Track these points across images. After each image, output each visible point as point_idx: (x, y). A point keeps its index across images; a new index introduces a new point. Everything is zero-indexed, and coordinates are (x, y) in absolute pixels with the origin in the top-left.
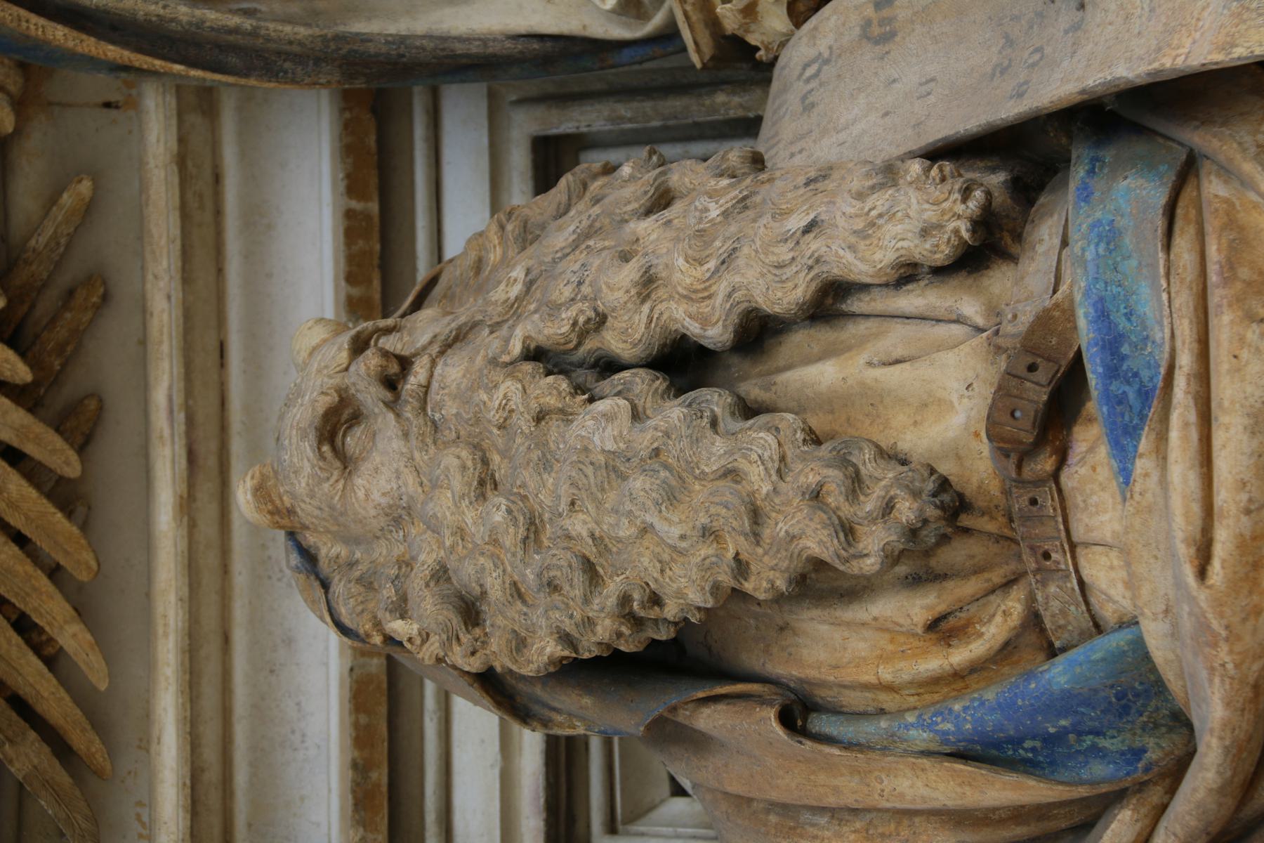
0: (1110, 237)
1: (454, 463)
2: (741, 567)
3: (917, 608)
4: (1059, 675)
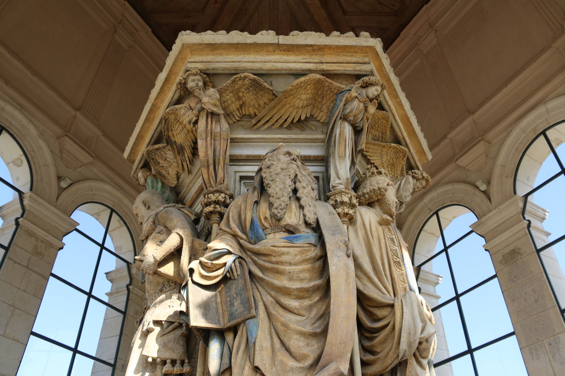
0: (308, 237)
1: (285, 166)
2: (273, 197)
3: (268, 216)
4: (261, 231)
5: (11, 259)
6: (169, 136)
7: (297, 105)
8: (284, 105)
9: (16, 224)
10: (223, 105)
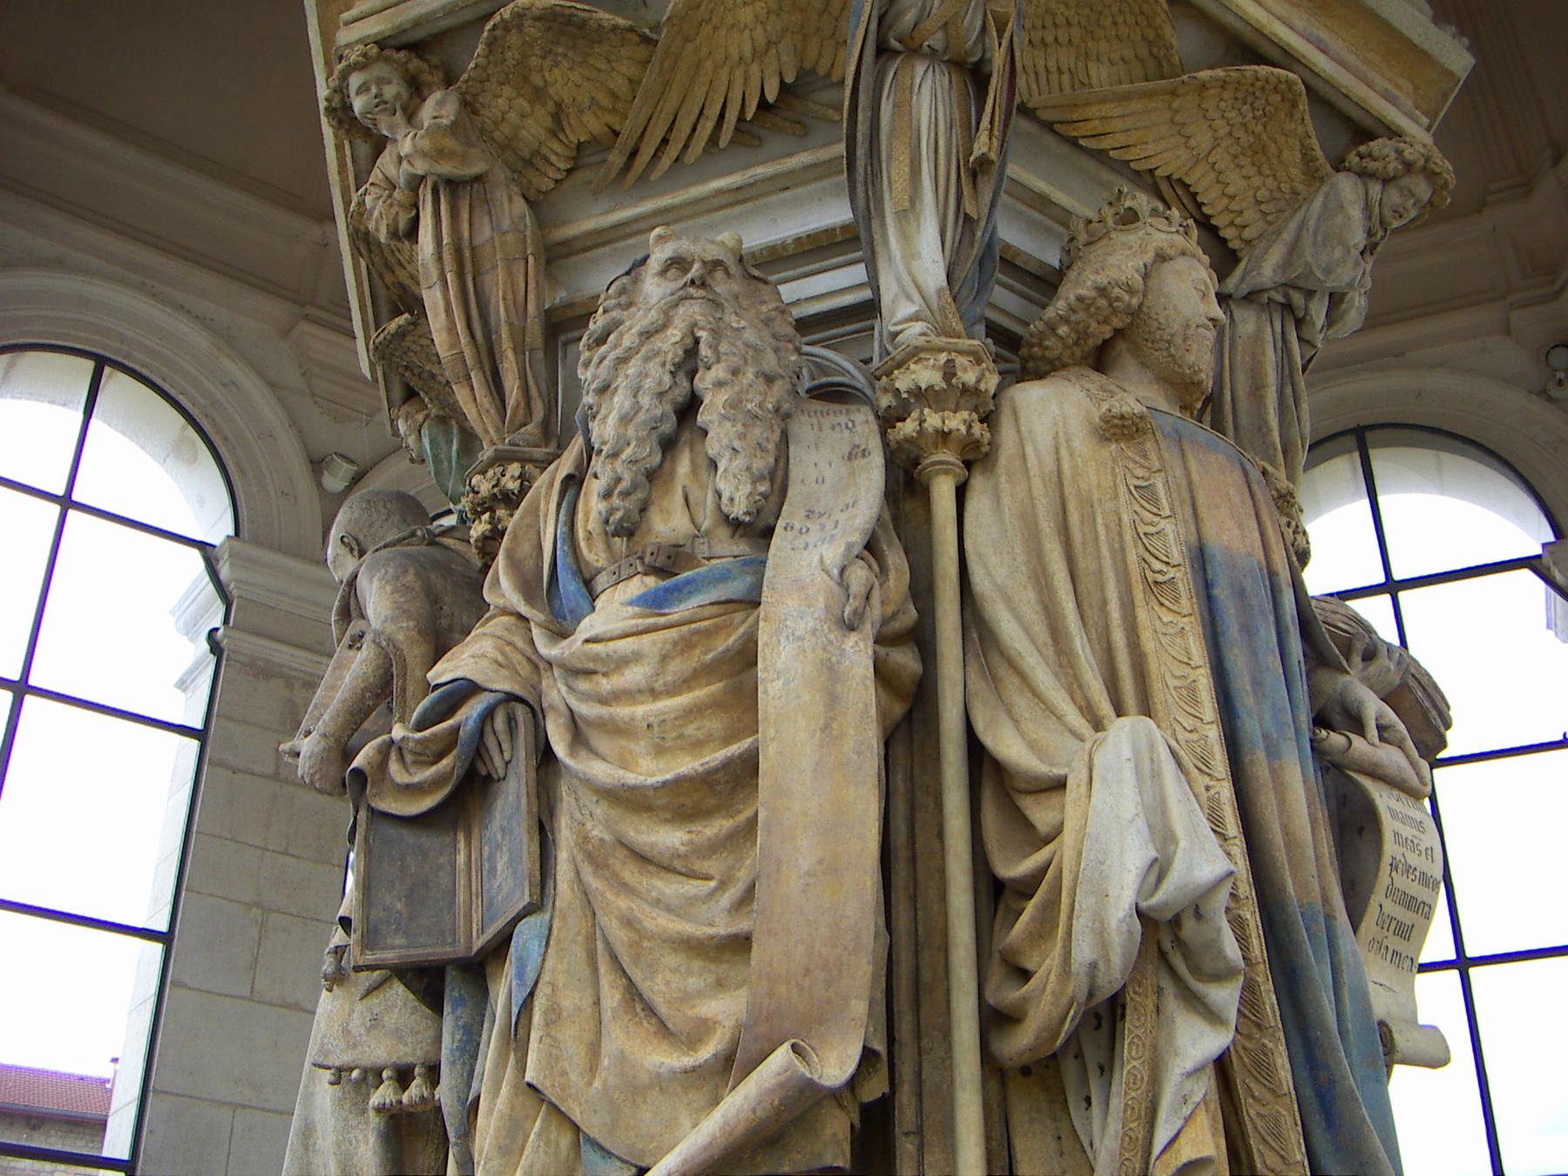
5: (222, 764)
6: (401, 286)
7: (734, 53)
8: (698, 66)
9: (212, 651)
10: (497, 134)
